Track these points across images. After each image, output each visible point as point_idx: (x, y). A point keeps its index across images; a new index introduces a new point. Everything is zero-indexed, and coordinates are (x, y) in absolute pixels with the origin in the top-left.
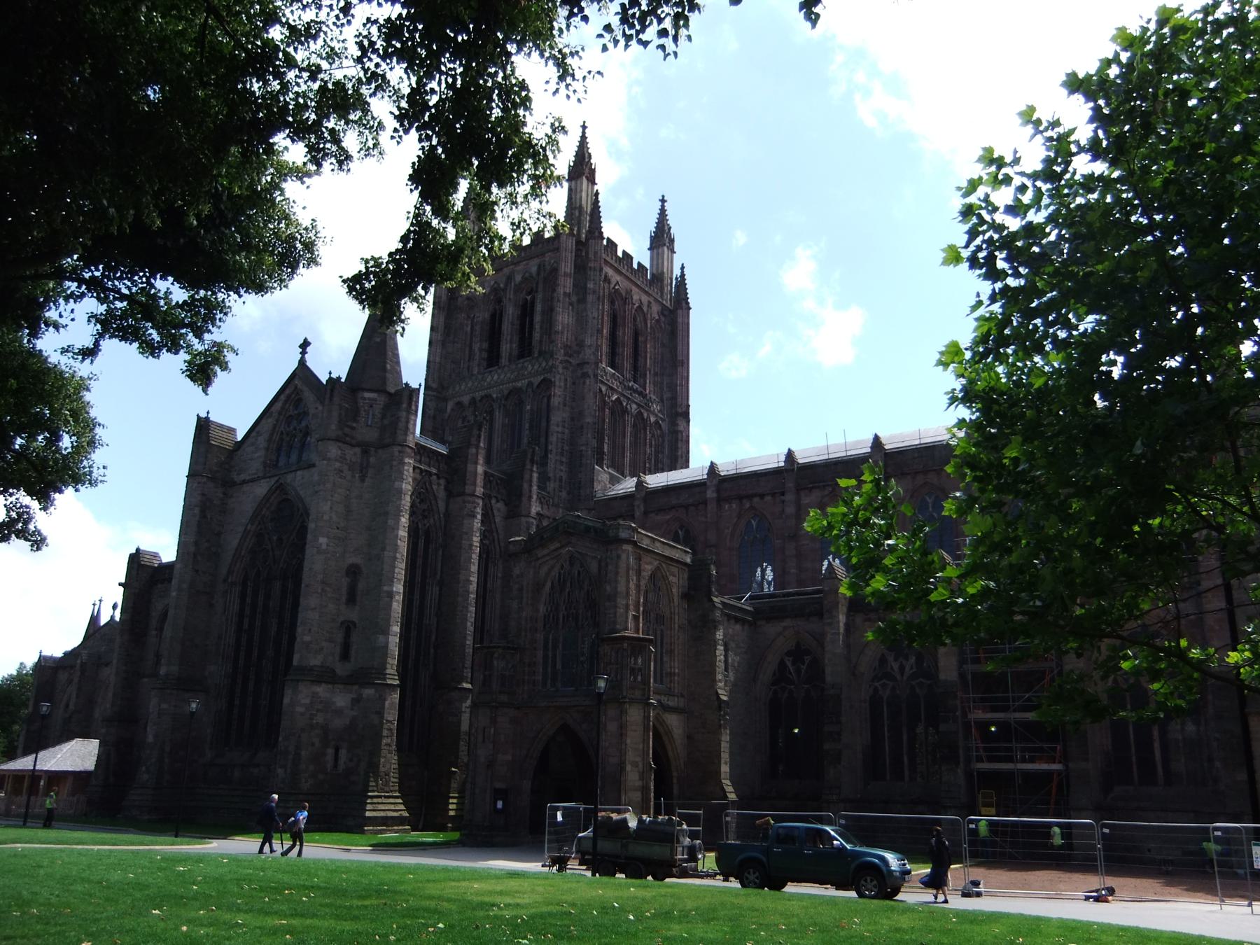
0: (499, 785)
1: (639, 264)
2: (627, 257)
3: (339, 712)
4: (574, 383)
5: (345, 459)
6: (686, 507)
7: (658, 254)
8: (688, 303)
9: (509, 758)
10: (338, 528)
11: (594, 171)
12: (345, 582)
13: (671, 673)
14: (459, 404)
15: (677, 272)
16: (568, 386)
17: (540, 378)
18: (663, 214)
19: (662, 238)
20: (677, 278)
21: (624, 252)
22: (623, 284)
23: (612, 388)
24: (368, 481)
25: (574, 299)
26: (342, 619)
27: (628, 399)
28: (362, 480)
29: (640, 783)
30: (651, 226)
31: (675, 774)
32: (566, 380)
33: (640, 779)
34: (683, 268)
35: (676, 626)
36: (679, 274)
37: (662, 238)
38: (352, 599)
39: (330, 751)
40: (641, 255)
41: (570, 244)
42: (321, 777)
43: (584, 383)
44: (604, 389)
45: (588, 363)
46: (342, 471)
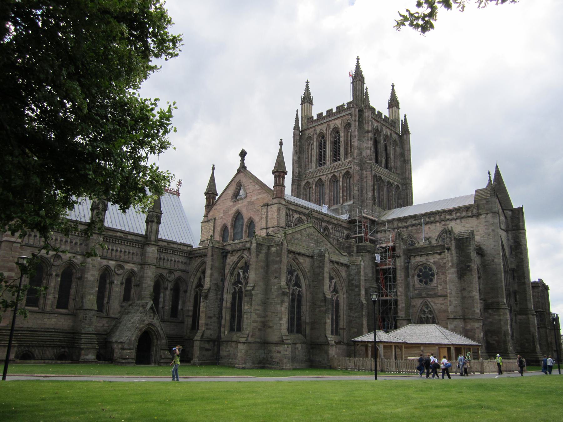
1: (385, 116)
2: (380, 114)
7: (392, 110)
8: (409, 132)
11: (363, 78)
14: (308, 182)
15: (402, 117)
17: (345, 171)
18: (393, 90)
19: (394, 103)
20: (402, 121)
21: (378, 112)
22: (380, 126)
30: (388, 97)
34: (405, 116)
36: (403, 119)
37: (394, 103)
40: (385, 112)
41: (355, 111)
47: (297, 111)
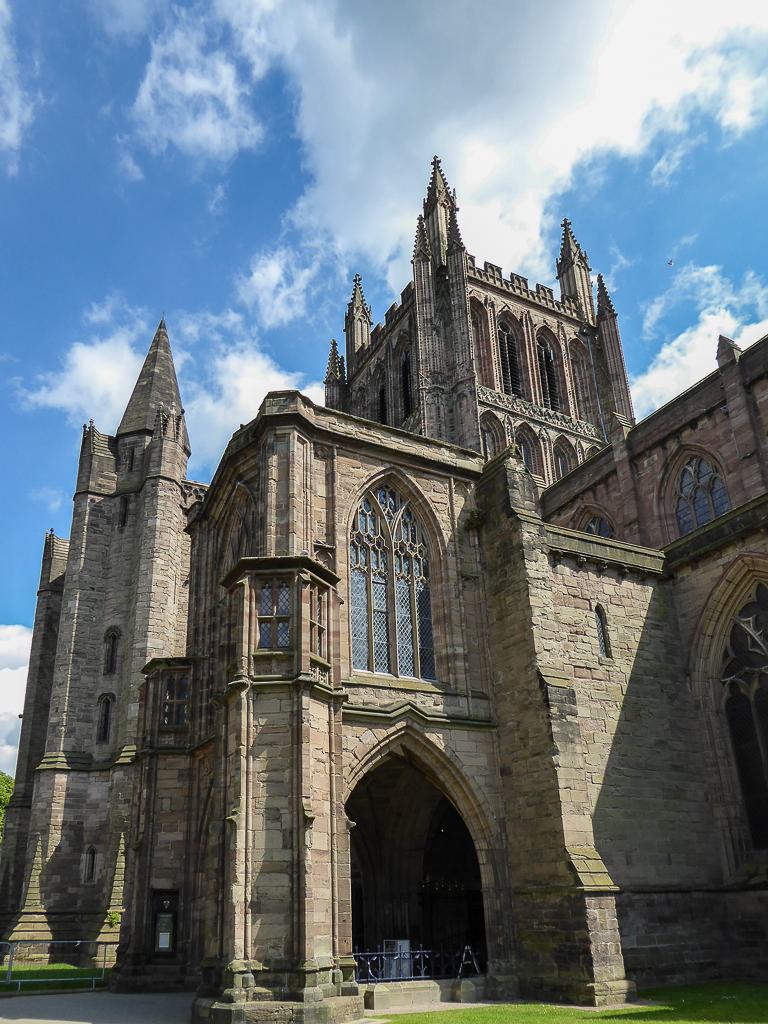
0: (161, 883)
3: (95, 806)
4: (451, 411)
5: (101, 512)
6: (592, 488)
9: (179, 836)
10: (93, 589)
12: (104, 648)
13: (448, 657)
16: (442, 414)
23: (514, 414)
24: (128, 530)
25: (439, 323)
26: (99, 692)
27: (541, 424)
28: (121, 531)
29: (286, 855)
31: (480, 845)
32: (439, 408)
33: (285, 847)
35: (453, 574)
38: (110, 669)
39: (84, 857)
42: (71, 890)
43: (461, 404)
44: (500, 415)
45: (462, 382)
46: (97, 526)
47: (335, 344)
